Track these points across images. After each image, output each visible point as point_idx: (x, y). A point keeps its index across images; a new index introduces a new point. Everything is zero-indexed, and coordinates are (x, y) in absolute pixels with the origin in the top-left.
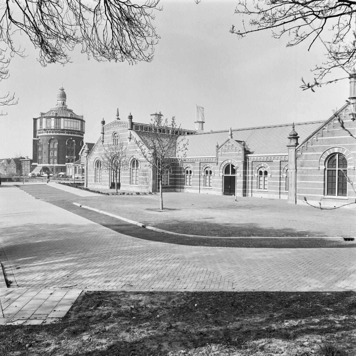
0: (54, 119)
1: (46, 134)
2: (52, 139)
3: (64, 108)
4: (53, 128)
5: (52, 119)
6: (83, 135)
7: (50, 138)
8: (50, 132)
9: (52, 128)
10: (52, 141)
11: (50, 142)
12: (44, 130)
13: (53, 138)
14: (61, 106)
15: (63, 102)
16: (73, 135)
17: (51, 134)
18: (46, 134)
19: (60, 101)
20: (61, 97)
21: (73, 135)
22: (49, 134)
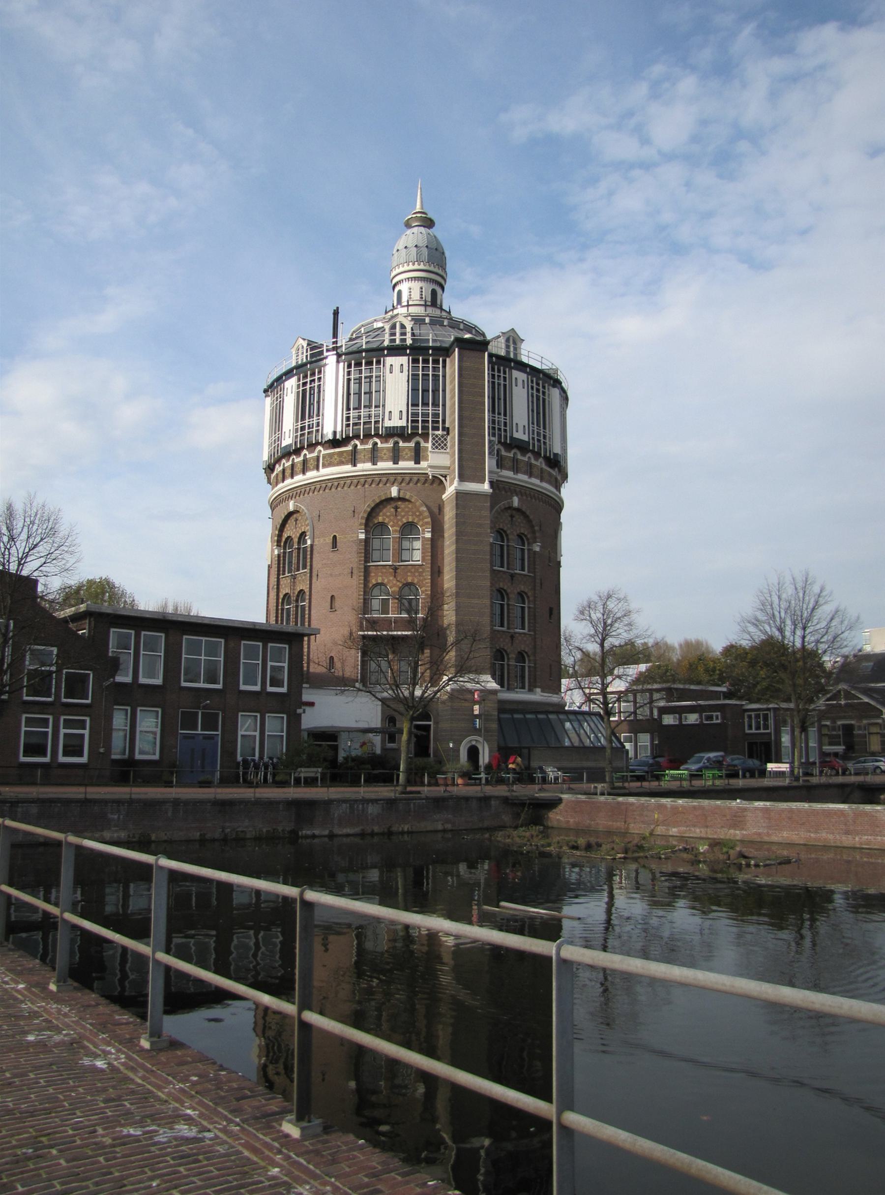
0: (404, 360)
1: (346, 469)
2: (390, 500)
4: (396, 422)
5: (390, 360)
6: (558, 487)
7: (375, 494)
9: (388, 423)
10: (385, 516)
11: (372, 523)
12: (335, 443)
13: (394, 492)
14: (419, 311)
15: (434, 293)
16: (522, 478)
17: (385, 466)
19: (416, 286)
20: (419, 261)
21: (522, 478)
22: (364, 467)
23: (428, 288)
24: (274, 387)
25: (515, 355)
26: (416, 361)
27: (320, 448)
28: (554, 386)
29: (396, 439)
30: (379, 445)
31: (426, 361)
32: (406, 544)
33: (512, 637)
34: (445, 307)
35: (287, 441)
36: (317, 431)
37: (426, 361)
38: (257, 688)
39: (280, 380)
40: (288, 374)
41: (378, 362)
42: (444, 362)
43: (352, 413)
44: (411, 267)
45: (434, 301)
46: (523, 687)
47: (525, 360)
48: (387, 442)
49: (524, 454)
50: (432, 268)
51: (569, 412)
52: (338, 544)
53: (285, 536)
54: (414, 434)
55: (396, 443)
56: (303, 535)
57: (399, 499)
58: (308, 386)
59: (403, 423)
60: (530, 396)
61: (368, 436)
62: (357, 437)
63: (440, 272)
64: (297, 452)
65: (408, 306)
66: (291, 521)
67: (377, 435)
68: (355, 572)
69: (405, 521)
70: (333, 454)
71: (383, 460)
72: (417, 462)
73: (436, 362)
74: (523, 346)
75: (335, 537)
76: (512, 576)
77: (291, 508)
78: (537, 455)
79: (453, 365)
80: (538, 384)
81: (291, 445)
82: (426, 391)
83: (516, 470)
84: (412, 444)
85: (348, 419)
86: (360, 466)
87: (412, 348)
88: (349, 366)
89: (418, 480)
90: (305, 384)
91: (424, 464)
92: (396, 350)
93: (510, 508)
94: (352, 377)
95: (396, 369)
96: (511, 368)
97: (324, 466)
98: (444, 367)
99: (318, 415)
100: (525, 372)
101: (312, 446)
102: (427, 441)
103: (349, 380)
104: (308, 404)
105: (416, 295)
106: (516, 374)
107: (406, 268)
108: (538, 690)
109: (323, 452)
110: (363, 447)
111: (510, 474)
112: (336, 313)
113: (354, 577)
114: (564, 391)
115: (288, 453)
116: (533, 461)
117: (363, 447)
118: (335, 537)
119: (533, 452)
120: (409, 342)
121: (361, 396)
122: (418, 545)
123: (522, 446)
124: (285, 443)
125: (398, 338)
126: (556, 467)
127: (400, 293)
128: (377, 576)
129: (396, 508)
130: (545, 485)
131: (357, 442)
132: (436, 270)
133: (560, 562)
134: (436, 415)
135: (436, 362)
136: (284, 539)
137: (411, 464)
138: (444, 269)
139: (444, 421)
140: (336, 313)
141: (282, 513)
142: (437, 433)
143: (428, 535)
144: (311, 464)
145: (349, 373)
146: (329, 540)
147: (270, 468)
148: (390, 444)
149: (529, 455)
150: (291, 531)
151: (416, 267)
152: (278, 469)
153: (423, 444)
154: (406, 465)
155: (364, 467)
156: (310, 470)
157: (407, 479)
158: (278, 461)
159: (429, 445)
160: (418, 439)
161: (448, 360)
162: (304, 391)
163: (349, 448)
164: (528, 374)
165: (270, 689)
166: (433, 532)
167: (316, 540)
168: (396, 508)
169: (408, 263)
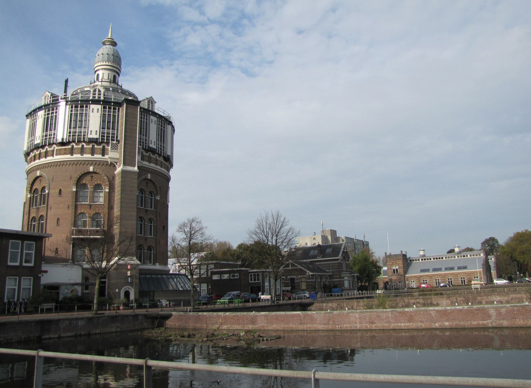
0: (99, 107)
1: (68, 157)
2: (89, 173)
3: (119, 90)
4: (94, 136)
5: (92, 106)
6: (168, 171)
7: (81, 170)
8: (82, 151)
9: (90, 136)
11: (80, 184)
12: (62, 144)
13: (91, 169)
15: (115, 77)
17: (87, 156)
18: (68, 157)
19: (106, 72)
20: (108, 61)
22: (77, 156)
23: (112, 74)
24: (32, 114)
25: (152, 108)
26: (105, 108)
27: (55, 146)
28: (169, 124)
29: (93, 144)
30: (85, 146)
31: (110, 108)
32: (96, 194)
33: (146, 239)
34: (120, 84)
35: (38, 141)
36: (54, 137)
37: (110, 108)
38: (18, 264)
39: (35, 111)
40: (40, 108)
41: (86, 107)
42: (119, 109)
43: (72, 130)
44: (104, 63)
45: (114, 80)
46: (151, 263)
47: (156, 111)
48: (89, 145)
49: (154, 155)
50: (114, 65)
51: (175, 136)
52: (62, 193)
53: (34, 188)
54: (102, 142)
55: (93, 146)
56: (44, 188)
57: (94, 172)
58: (50, 115)
59: (97, 136)
60: (158, 128)
61: (79, 141)
62: (74, 141)
63: (118, 67)
64: (43, 147)
65: (102, 81)
66: (38, 181)
67: (84, 141)
68: (70, 207)
69: (96, 183)
70: (62, 149)
71: (86, 153)
72: (103, 155)
73: (115, 109)
74: (156, 105)
75: (60, 190)
76: (146, 211)
77: (38, 174)
78: (160, 155)
79: (123, 111)
80: (162, 123)
81: (39, 144)
82: (109, 122)
83: (150, 162)
84: (101, 147)
85: (70, 133)
86: (75, 156)
87: (103, 101)
88: (72, 107)
89: (103, 164)
90: (48, 114)
91: (106, 157)
92: (96, 102)
93: (146, 179)
94: (73, 113)
95: (95, 110)
96: (150, 115)
97: (56, 155)
98: (118, 111)
99: (55, 130)
100: (156, 117)
101: (50, 145)
102: (108, 146)
103: (71, 114)
104: (50, 124)
105: (106, 77)
106: (152, 117)
107: (102, 64)
108: (158, 264)
109: (56, 148)
110: (77, 147)
111: (147, 163)
112: (67, 81)
113: (70, 209)
114: (173, 127)
115: (37, 147)
116: (158, 158)
117: (77, 147)
118: (60, 190)
119: (158, 154)
120: (102, 98)
121: (77, 121)
122: (102, 195)
123: (153, 151)
124: (36, 142)
125: (97, 96)
126: (168, 161)
127: (98, 75)
128: (81, 209)
129: (92, 177)
130: (162, 169)
131: (74, 144)
132: (116, 66)
133: (168, 205)
134: (113, 134)
135: (115, 109)
136: (33, 190)
137: (100, 156)
138: (120, 66)
139: (117, 137)
140: (67, 81)
141: (32, 177)
142: (113, 142)
143: (107, 190)
144: (50, 153)
145: (72, 111)
146: (57, 191)
147: (27, 154)
148: (90, 146)
149: (156, 155)
150: (37, 186)
151: (107, 63)
152: (32, 155)
153: (106, 147)
154: (98, 156)
155: (77, 156)
156: (49, 156)
157: (98, 163)
158: (32, 151)
159: (110, 148)
160: (104, 144)
161: (120, 108)
162: (48, 118)
163: (70, 147)
164: (157, 118)
165: (24, 264)
166: (109, 189)
167: (51, 191)
168: (92, 177)
169: (103, 61)
